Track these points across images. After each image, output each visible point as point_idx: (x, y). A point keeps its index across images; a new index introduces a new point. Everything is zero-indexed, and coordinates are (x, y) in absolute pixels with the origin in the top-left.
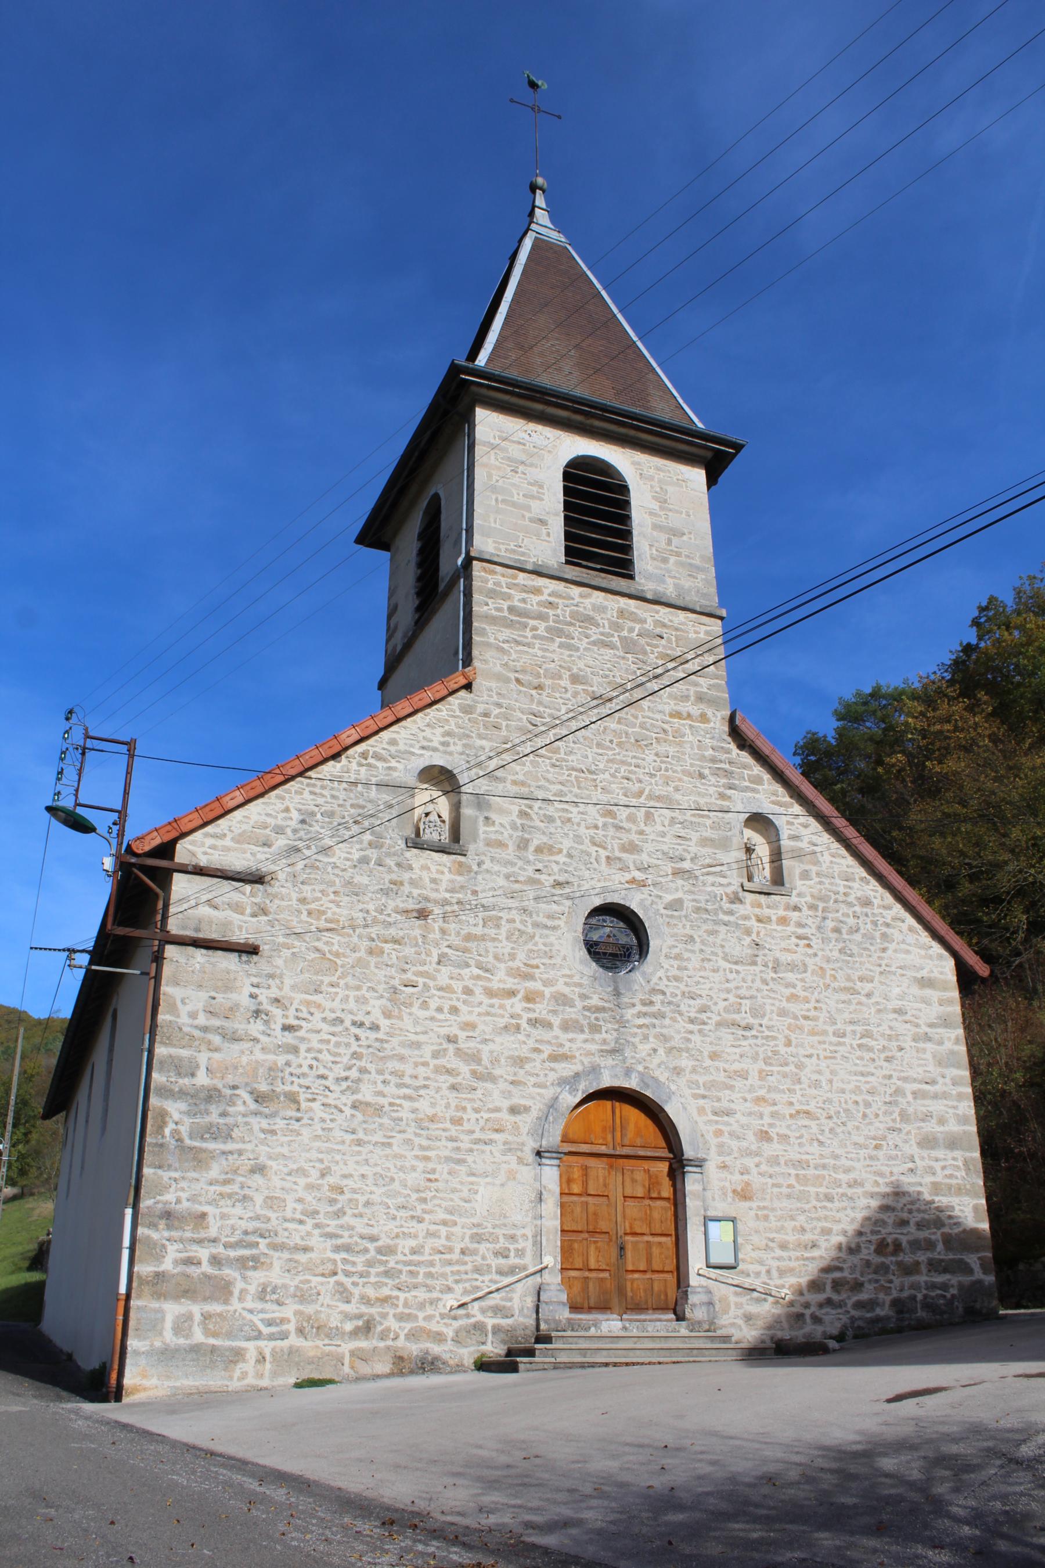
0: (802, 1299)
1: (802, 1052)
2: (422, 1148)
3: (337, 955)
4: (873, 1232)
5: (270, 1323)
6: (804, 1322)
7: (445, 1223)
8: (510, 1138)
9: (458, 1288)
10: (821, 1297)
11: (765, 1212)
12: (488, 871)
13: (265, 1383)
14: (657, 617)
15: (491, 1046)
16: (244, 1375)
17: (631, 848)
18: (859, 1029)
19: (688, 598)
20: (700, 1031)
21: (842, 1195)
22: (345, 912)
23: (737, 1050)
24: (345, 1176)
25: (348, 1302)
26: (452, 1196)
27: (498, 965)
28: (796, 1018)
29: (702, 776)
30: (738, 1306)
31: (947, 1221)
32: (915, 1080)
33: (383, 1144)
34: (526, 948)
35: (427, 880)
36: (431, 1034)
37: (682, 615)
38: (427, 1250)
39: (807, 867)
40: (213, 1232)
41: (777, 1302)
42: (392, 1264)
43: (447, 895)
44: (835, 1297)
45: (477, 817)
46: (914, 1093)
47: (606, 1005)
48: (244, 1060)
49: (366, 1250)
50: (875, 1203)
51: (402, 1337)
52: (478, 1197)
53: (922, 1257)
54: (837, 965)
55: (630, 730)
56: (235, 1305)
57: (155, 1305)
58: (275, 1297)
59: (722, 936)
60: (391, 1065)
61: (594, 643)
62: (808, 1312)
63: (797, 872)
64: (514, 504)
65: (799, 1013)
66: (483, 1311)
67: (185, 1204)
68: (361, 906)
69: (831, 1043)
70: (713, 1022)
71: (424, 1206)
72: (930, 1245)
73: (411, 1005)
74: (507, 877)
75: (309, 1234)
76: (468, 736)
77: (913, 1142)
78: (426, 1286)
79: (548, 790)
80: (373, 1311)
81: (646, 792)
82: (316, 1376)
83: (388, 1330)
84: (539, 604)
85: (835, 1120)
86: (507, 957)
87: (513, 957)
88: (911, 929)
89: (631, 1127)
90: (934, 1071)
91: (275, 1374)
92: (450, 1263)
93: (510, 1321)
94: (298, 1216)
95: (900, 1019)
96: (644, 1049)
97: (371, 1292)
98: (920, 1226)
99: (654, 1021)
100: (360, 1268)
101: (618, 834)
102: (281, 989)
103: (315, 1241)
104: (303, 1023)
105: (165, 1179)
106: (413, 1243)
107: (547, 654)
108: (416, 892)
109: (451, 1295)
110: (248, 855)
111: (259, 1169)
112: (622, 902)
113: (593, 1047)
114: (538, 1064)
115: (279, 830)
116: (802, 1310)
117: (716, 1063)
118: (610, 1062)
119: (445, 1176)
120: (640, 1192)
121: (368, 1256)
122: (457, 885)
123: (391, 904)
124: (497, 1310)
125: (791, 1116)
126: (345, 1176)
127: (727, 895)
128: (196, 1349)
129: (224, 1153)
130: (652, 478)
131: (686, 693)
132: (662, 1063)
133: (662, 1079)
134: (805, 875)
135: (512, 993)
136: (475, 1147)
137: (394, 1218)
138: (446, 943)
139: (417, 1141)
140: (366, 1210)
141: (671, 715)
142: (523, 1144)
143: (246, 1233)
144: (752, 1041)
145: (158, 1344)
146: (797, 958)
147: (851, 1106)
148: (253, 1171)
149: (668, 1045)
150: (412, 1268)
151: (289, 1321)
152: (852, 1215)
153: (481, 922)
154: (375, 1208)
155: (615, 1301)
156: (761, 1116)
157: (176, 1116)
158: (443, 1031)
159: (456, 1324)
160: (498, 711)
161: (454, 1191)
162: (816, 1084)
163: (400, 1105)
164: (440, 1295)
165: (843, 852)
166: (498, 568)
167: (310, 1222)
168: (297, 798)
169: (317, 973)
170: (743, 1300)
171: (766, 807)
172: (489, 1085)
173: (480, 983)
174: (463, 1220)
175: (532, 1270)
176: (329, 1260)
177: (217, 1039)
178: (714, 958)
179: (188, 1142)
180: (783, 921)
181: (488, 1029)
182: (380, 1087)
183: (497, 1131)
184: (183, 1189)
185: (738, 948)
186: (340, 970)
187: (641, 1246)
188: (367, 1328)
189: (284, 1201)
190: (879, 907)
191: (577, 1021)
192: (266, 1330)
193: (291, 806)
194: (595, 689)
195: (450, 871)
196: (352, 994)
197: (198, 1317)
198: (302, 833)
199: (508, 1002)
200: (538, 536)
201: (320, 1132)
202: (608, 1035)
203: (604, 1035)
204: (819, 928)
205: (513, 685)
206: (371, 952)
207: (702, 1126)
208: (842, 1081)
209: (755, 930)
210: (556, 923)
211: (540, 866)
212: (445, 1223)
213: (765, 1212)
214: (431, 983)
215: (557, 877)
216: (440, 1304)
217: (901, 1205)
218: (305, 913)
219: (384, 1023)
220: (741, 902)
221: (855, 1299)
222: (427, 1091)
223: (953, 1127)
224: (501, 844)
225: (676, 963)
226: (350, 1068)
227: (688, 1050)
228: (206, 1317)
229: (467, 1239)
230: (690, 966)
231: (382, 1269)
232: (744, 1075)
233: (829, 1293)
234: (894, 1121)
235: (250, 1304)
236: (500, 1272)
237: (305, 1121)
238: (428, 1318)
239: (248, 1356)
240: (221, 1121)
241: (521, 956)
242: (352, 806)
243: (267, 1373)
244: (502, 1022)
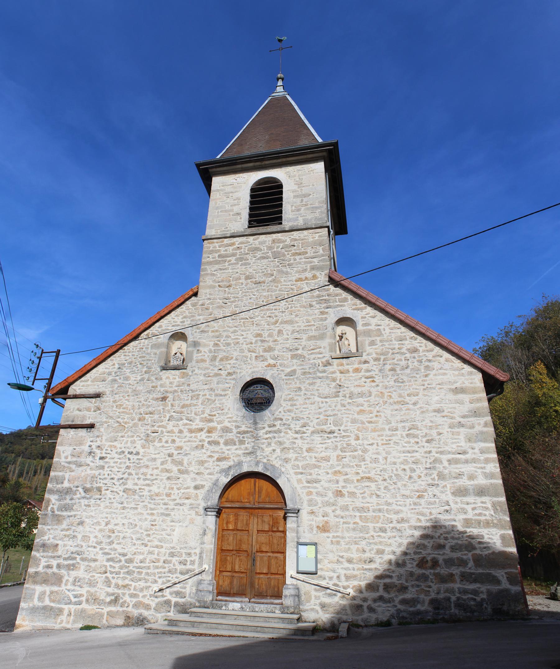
0: (362, 596)
1: (366, 442)
2: (151, 509)
3: (126, 423)
4: (415, 553)
5: (75, 596)
6: (363, 611)
7: (157, 547)
8: (193, 502)
9: (160, 581)
10: (376, 595)
11: (338, 539)
12: (196, 374)
13: (69, 626)
14: (292, 237)
15: (189, 456)
16: (62, 622)
17: (270, 349)
18: (407, 425)
19: (309, 223)
20: (301, 437)
21: (393, 528)
22: (131, 403)
23: (324, 446)
24: (116, 525)
25: (110, 587)
26: (162, 533)
27: (196, 417)
28: (363, 423)
29: (311, 306)
30: (317, 598)
31: (477, 546)
32: (449, 453)
33: (134, 508)
34: (210, 407)
35: (168, 383)
36: (162, 454)
37: (305, 232)
38: (148, 561)
39: (373, 339)
40: (59, 553)
41: (343, 597)
42: (131, 568)
43: (176, 388)
44: (386, 595)
45: (193, 351)
46: (449, 461)
47: (249, 430)
48: (83, 474)
49: (120, 561)
50: (417, 533)
51: (131, 606)
52: (175, 533)
53: (456, 571)
54: (392, 389)
56: (63, 587)
57: (33, 587)
58: (79, 583)
59: (318, 384)
60: (143, 470)
61: (258, 259)
62: (365, 605)
63: (367, 343)
64: (226, 211)
65: (365, 420)
66: (171, 594)
67: (51, 540)
68: (138, 400)
69: (387, 436)
70: (310, 432)
71: (149, 538)
72: (463, 563)
73: (154, 441)
74: (205, 375)
75: (97, 553)
76: (193, 316)
77: (448, 492)
78: (145, 579)
79: (228, 331)
80: (120, 592)
81: (280, 321)
82: (91, 624)
83: (125, 602)
85: (388, 481)
86: (200, 413)
87: (203, 412)
88: (447, 360)
89: (264, 492)
90: (464, 445)
91: (74, 622)
92: (157, 567)
93: (183, 600)
94: (94, 545)
95: (439, 415)
96: (268, 450)
97: (120, 582)
98: (453, 549)
99: (275, 435)
100: (117, 570)
101: (263, 344)
102: (101, 441)
103: (100, 557)
104: (108, 455)
105: (46, 529)
106: (141, 557)
108: (162, 389)
109: (156, 585)
110: (96, 387)
111: (81, 523)
112: (261, 377)
113: (240, 452)
114: (211, 463)
115: (109, 374)
116: (361, 603)
117: (310, 454)
118: (248, 459)
119: (160, 523)
120: (266, 528)
121: (121, 564)
122: (181, 383)
123: (151, 396)
124: (178, 594)
125: (358, 481)
126: (116, 525)
127: (322, 362)
128: (45, 608)
129: (69, 516)
130: (295, 176)
131: (305, 268)
132: (278, 456)
133: (277, 465)
134: (372, 343)
135: (202, 430)
136: (176, 507)
137: (135, 545)
138: (173, 411)
139: (149, 506)
140: (122, 541)
141: (296, 281)
142: (199, 505)
143: (72, 553)
144: (333, 440)
145: (31, 605)
146: (365, 390)
147: (400, 472)
148: (79, 524)
149: (282, 447)
150: (140, 570)
151: (83, 596)
152: (400, 541)
153: (190, 398)
154: (127, 540)
155: (248, 590)
156: (337, 482)
157: (53, 501)
158: (168, 452)
159: (157, 600)
160: (209, 301)
161: (164, 530)
162: (376, 460)
163: (144, 489)
164: (151, 585)
165: (399, 325)
166: (215, 240)
167: (99, 547)
168: (118, 359)
169: (116, 433)
170: (321, 594)
171: (349, 313)
172: (185, 476)
173: (187, 427)
174: (166, 545)
175: (197, 571)
176: (104, 566)
177: (73, 467)
178: (312, 397)
179: (56, 512)
180: (357, 370)
181: (188, 449)
182: (136, 481)
183: (187, 498)
184: (51, 534)
185: (327, 389)
186: (126, 429)
187: (265, 558)
188: (115, 601)
189: (89, 537)
190: (424, 351)
191: (233, 440)
192: (74, 600)
193: (116, 363)
195: (179, 378)
196: (130, 439)
197: (48, 593)
198: (118, 373)
199: (199, 435)
201: (108, 504)
202: (249, 445)
203: (247, 445)
204: (380, 370)
205: (217, 289)
206: (140, 420)
207: (300, 491)
208: (394, 457)
209: (338, 378)
210: (227, 392)
211: (221, 367)
212: (157, 547)
213: (338, 539)
214: (164, 430)
215: (229, 371)
216: (151, 589)
217: (438, 534)
218: (115, 406)
219: (141, 451)
220: (330, 364)
221: (401, 597)
222: (157, 481)
223: (481, 481)
224: (203, 361)
225: (289, 403)
226: (124, 474)
227: (293, 448)
228: (52, 592)
229: (167, 555)
230: (298, 403)
231: (126, 570)
232: (327, 459)
233: (381, 592)
234: (433, 479)
235: (69, 587)
236: (182, 573)
237: (102, 500)
238: (144, 596)
239: (64, 612)
240: (70, 502)
241: (208, 411)
242: (140, 357)
243: (71, 621)
244: (195, 444)
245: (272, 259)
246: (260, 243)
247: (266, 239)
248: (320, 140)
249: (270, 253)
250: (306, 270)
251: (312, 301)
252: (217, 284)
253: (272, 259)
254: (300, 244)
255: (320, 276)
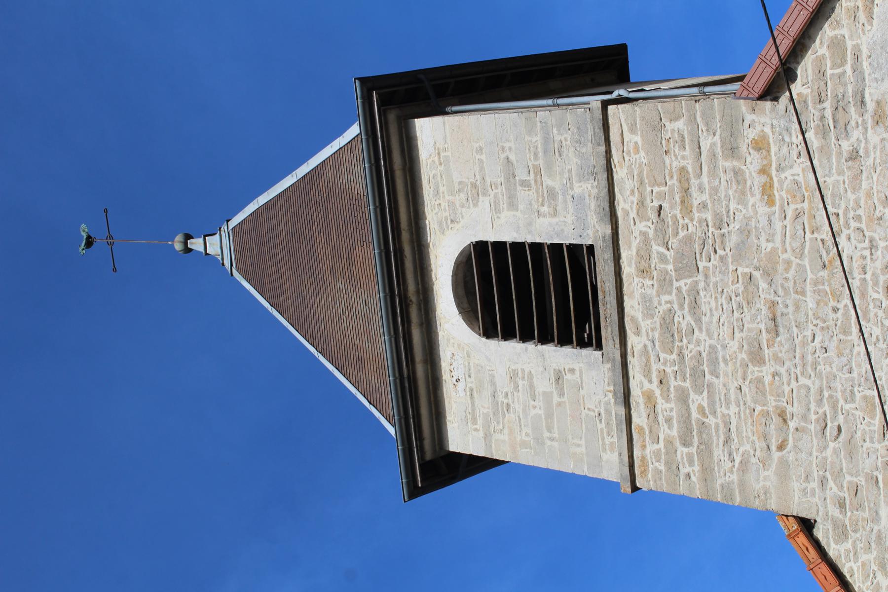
14: (633, 214)
19: (593, 162)
29: (854, 156)
37: (619, 174)
55: (810, 276)
61: (698, 321)
64: (549, 416)
84: (667, 399)
107: (733, 397)
130: (451, 204)
131: (730, 175)
141: (771, 202)
160: (831, 484)
166: (637, 453)
194: (762, 326)
200: (580, 386)
245: (701, 277)
246: (649, 313)
247: (637, 295)
248: (354, 130)
249: (682, 283)
250: (737, 173)
251: (840, 153)
252: (776, 455)
253: (701, 277)
254: (656, 189)
255: (759, 128)
